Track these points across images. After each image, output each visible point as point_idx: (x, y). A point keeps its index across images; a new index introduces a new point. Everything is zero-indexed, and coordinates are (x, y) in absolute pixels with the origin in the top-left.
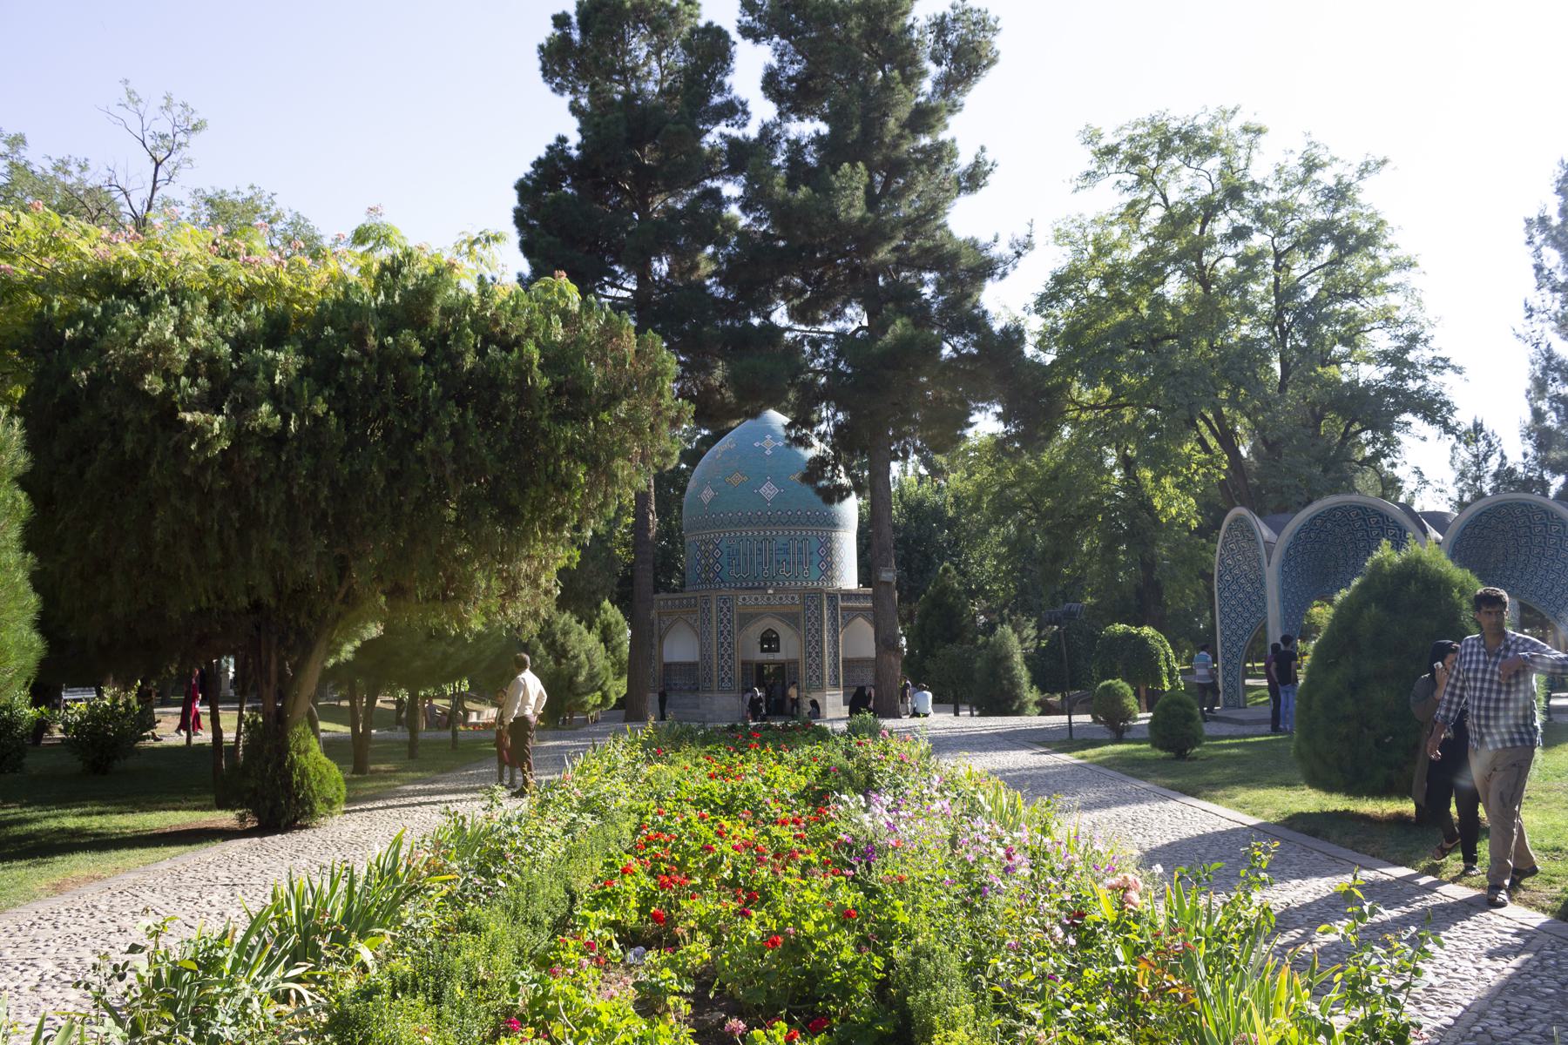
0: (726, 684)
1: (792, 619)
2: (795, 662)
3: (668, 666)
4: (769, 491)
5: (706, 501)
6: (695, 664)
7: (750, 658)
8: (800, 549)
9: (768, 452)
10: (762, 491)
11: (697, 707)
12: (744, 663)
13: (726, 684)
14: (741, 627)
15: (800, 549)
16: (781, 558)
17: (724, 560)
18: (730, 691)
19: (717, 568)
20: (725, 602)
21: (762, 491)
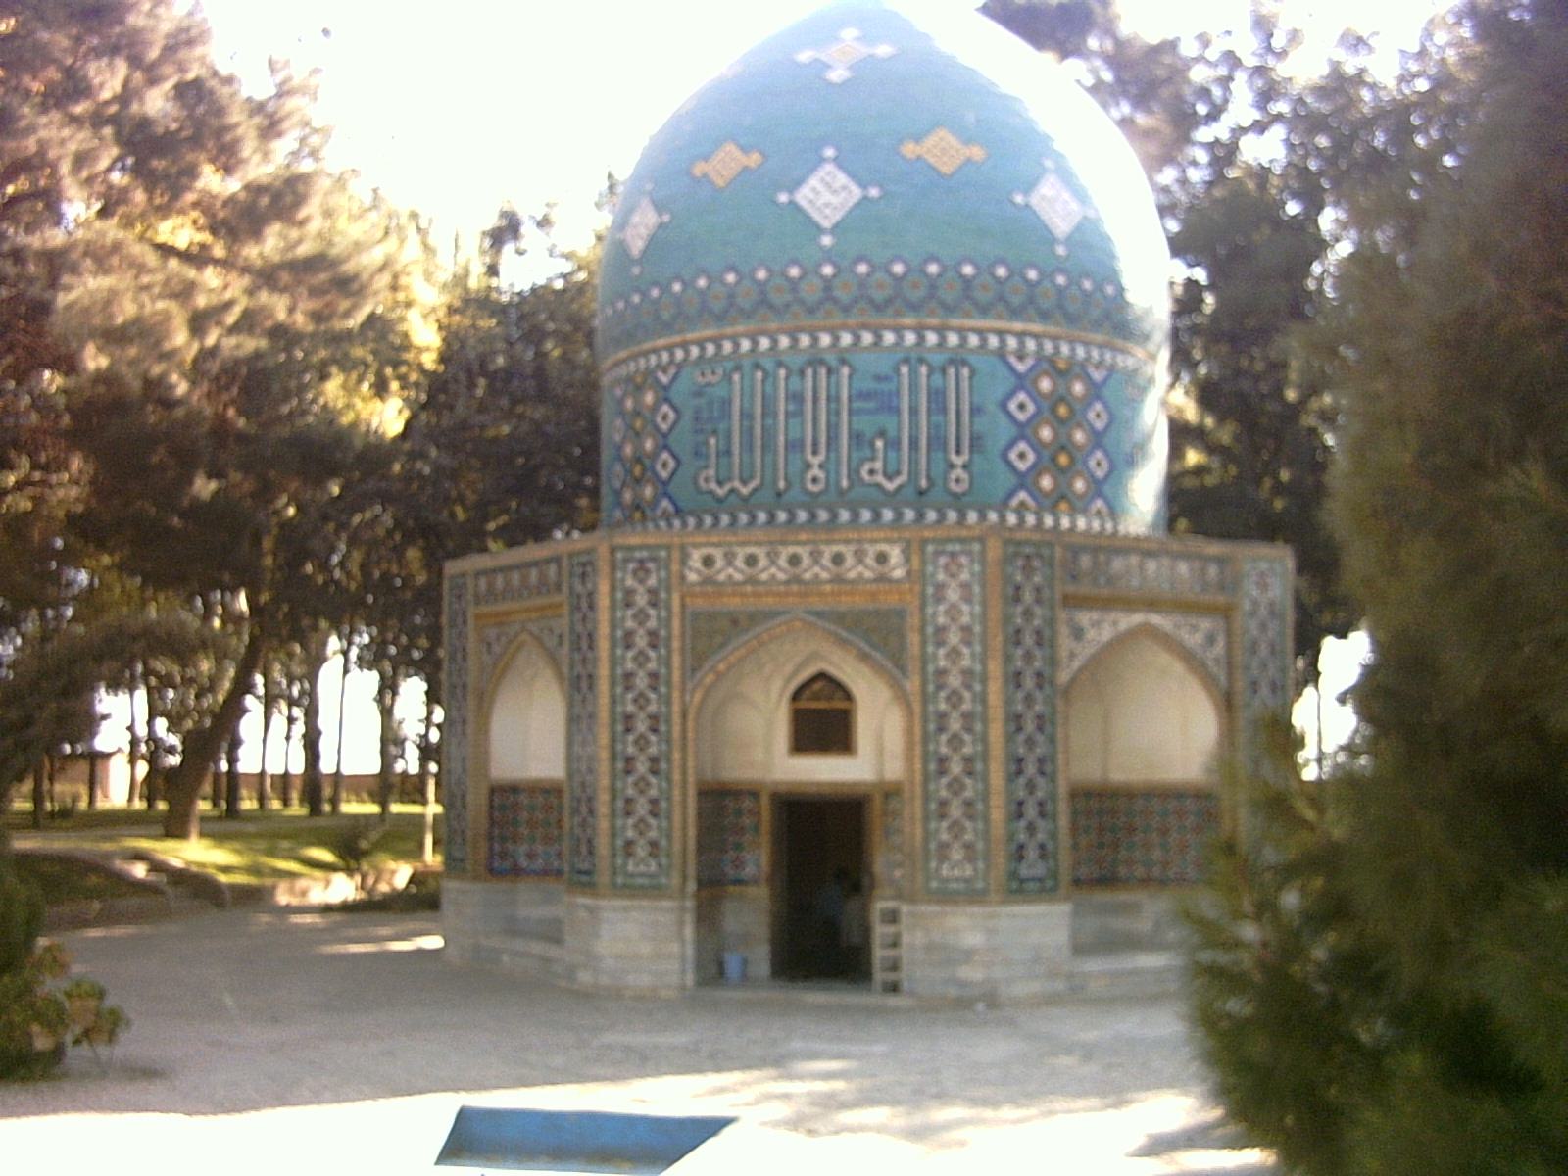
0: (641, 865)
2: (891, 792)
4: (828, 194)
5: (637, 246)
7: (739, 769)
8: (937, 398)
9: (837, 75)
10: (803, 196)
11: (553, 933)
13: (641, 865)
14: (696, 661)
15: (937, 398)
16: (866, 425)
17: (683, 440)
18: (652, 890)
21: (803, 196)
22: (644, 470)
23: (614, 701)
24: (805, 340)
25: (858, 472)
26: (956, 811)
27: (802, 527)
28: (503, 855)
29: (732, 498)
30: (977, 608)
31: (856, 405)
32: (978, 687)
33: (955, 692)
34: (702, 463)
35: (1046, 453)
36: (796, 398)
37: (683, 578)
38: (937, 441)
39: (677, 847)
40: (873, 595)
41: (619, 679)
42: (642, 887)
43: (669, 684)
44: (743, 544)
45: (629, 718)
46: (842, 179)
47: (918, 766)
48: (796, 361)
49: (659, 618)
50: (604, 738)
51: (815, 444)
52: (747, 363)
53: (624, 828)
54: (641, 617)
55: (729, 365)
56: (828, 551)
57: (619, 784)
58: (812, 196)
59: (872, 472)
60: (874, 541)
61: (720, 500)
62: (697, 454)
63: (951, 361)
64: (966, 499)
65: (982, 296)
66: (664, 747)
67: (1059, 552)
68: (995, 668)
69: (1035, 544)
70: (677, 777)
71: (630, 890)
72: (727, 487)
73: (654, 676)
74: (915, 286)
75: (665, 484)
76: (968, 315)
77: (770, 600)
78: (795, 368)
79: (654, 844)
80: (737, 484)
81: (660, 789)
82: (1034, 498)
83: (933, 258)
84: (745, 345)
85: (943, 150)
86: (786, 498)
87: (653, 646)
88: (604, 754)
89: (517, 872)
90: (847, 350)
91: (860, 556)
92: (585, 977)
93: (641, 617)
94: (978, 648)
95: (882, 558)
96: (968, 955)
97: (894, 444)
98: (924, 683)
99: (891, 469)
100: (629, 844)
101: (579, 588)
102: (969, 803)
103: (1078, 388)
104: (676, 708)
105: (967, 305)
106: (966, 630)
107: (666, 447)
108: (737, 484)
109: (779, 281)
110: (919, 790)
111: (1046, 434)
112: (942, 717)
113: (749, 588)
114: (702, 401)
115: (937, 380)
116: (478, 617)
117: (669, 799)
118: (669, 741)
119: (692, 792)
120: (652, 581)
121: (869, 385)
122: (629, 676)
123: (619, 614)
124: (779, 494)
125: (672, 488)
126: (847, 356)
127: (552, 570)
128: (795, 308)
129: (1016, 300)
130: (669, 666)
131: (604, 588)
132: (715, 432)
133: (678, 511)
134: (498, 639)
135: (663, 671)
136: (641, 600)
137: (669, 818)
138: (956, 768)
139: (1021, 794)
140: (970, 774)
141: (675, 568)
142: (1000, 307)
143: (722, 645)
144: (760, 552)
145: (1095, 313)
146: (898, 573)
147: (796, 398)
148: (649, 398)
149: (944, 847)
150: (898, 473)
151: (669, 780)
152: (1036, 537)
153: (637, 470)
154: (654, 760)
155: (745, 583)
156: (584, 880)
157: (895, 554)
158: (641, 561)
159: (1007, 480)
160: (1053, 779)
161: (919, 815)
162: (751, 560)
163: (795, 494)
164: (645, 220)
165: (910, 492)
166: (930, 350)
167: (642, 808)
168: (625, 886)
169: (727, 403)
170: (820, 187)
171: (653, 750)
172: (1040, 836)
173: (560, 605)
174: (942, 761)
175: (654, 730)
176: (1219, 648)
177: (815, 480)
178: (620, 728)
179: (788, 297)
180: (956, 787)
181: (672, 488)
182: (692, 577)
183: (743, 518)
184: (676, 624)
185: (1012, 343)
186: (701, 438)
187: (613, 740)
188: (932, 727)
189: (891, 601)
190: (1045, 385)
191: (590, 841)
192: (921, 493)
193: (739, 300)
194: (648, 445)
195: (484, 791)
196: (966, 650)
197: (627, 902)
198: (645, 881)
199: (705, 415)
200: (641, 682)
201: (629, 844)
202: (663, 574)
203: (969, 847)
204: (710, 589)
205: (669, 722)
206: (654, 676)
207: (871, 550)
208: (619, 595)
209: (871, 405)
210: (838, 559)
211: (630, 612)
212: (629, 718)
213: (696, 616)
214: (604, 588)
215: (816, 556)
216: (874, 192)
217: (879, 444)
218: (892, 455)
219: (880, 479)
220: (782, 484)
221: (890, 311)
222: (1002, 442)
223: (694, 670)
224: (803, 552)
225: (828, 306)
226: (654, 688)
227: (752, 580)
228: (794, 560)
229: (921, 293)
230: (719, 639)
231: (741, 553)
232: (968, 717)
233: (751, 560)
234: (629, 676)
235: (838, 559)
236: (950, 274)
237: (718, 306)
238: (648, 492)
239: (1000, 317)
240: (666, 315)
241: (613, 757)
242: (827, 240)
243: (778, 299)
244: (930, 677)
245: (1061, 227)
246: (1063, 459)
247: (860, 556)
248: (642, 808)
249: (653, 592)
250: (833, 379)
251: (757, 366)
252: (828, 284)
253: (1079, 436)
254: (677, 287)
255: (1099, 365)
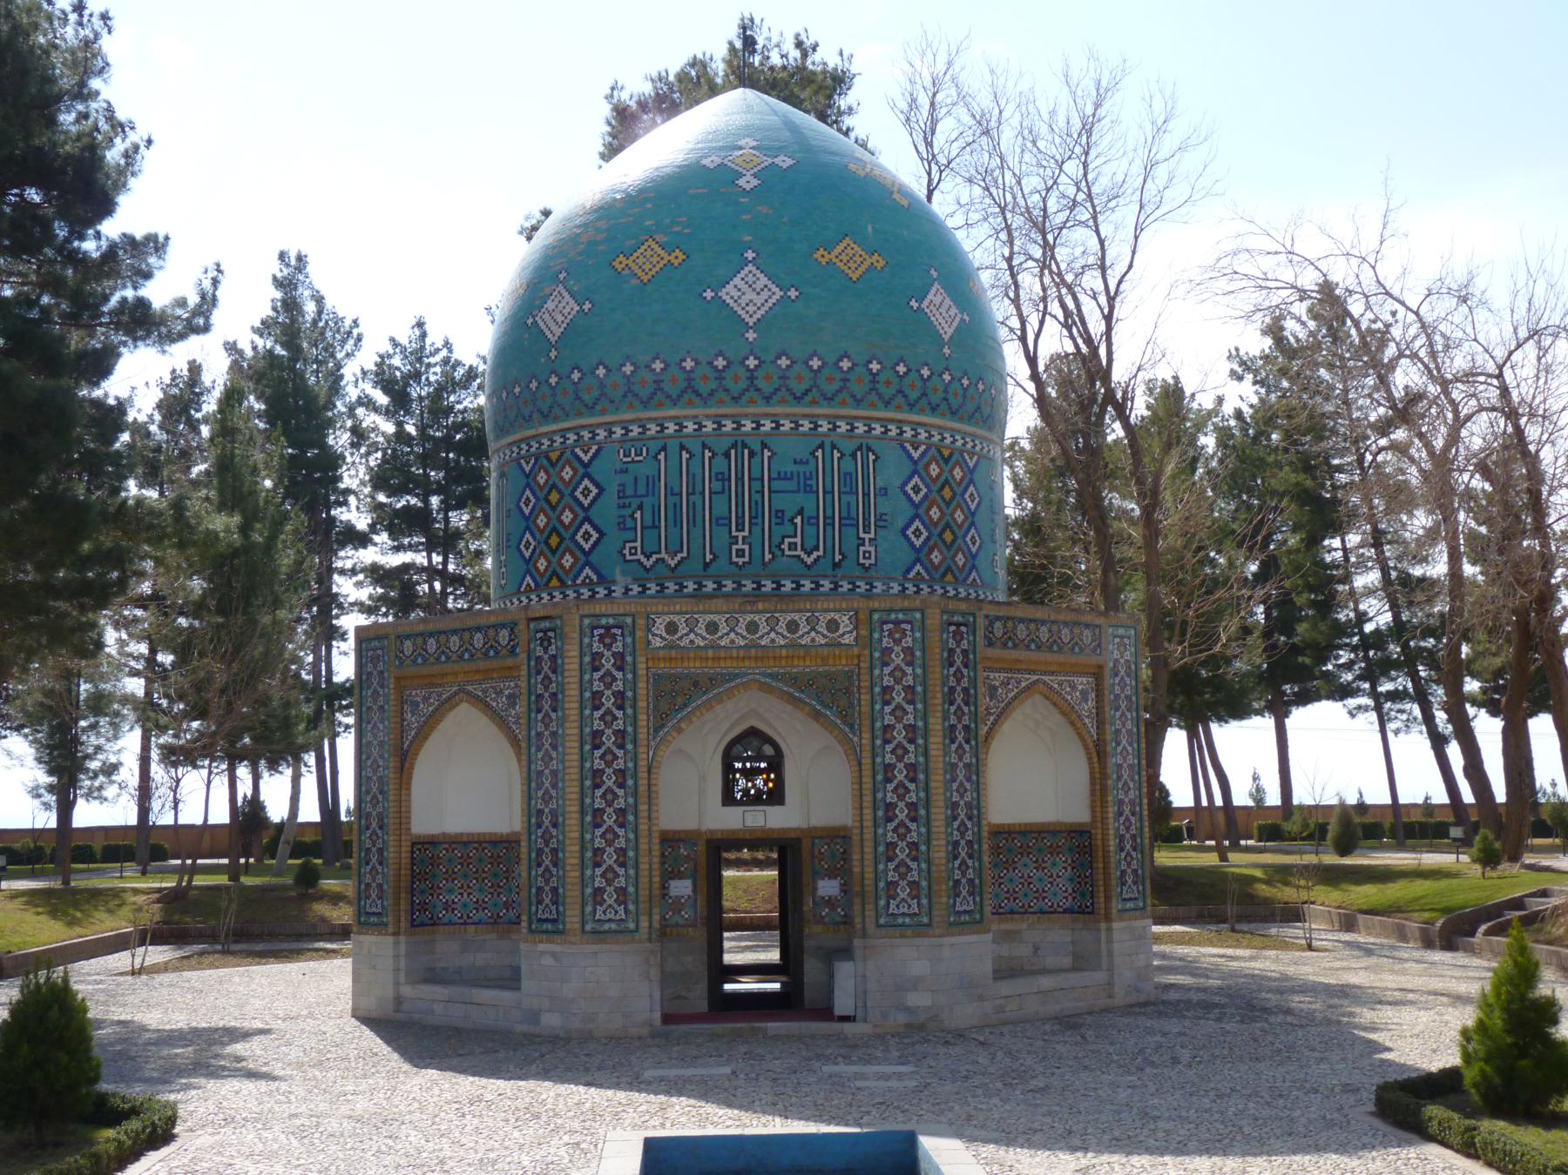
0: (610, 912)
1: (830, 695)
2: (837, 837)
3: (426, 847)
4: (750, 293)
5: (554, 332)
6: (507, 843)
8: (848, 478)
9: (748, 182)
10: (728, 293)
11: (511, 979)
12: (670, 840)
13: (610, 912)
15: (848, 478)
16: (788, 503)
17: (607, 512)
19: (585, 537)
20: (607, 635)
21: (728, 293)
22: (562, 539)
23: (582, 760)
24: (729, 426)
25: (779, 547)
26: (902, 853)
27: (710, 597)
28: (424, 907)
29: (660, 567)
30: (919, 671)
31: (777, 485)
32: (920, 741)
33: (899, 745)
34: (630, 535)
35: (936, 532)
36: (723, 478)
37: (649, 642)
38: (848, 520)
39: (644, 894)
40: (824, 660)
41: (588, 739)
42: (609, 931)
43: (635, 742)
44: (704, 613)
45: (597, 774)
46: (764, 280)
47: (868, 812)
48: (722, 444)
49: (625, 680)
50: (572, 791)
51: (740, 518)
52: (673, 446)
53: (593, 878)
54: (608, 679)
55: (655, 446)
56: (784, 619)
57: (588, 836)
58: (736, 294)
59: (793, 546)
60: (827, 611)
61: (647, 570)
62: (622, 526)
63: (860, 448)
64: (872, 573)
65: (888, 392)
66: (631, 800)
67: (981, 622)
68: (936, 724)
69: (963, 614)
70: (643, 827)
71: (599, 935)
72: (655, 557)
73: (621, 734)
74: (830, 380)
75: (587, 554)
76: (873, 406)
77: (729, 664)
78: (720, 450)
79: (622, 892)
80: (663, 555)
81: (627, 840)
82: (926, 570)
83: (846, 355)
84: (672, 428)
85: (850, 257)
86: (712, 570)
87: (621, 707)
88: (574, 808)
89: (434, 922)
90: (767, 434)
91: (813, 624)
92: (551, 1021)
93: (608, 679)
94: (920, 706)
95: (833, 625)
96: (915, 984)
97: (812, 521)
98: (873, 738)
99: (808, 546)
100: (598, 892)
101: (539, 652)
102: (913, 846)
103: (958, 473)
104: (643, 763)
105: (873, 397)
106: (910, 689)
107: (587, 519)
108: (663, 555)
109: (704, 369)
110: (868, 836)
111: (935, 513)
112: (889, 768)
113: (710, 653)
114: (627, 479)
115: (848, 465)
116: (398, 679)
117: (637, 849)
118: (635, 795)
119: (656, 840)
120: (618, 647)
121: (791, 468)
122: (597, 734)
123: (587, 677)
124: (706, 566)
125: (593, 558)
126: (768, 440)
127: (504, 635)
128: (722, 395)
129: (914, 395)
130: (635, 725)
131: (572, 652)
132: (640, 507)
133: (603, 580)
134: (425, 699)
135: (630, 729)
136: (608, 664)
137: (636, 867)
138: (902, 814)
139: (956, 836)
140: (914, 820)
141: (639, 634)
142: (900, 400)
143: (685, 706)
144: (721, 620)
145: (970, 406)
146: (847, 640)
147: (723, 478)
148: (567, 473)
149: (891, 885)
150: (817, 548)
151: (636, 832)
152: (963, 606)
153: (554, 541)
154: (621, 812)
155: (706, 647)
156: (552, 928)
157: (845, 623)
158: (608, 628)
159: (907, 556)
160: (979, 825)
161: (869, 856)
162: (712, 628)
163: (722, 561)
164: (560, 310)
165: (826, 565)
166: (842, 436)
167: (610, 859)
168: (594, 932)
169: (652, 482)
170: (741, 284)
171: (620, 803)
172: (970, 874)
173: (517, 668)
174: (890, 807)
175: (621, 786)
176: (1091, 704)
177: (740, 553)
178: (588, 783)
179: (713, 385)
180: (902, 830)
181: (593, 558)
182: (657, 642)
183: (672, 587)
184: (642, 685)
185: (909, 433)
186: (627, 512)
187: (582, 795)
188: (880, 777)
189: (842, 665)
190: (934, 470)
191: (555, 890)
192: (836, 566)
193: (666, 386)
194: (567, 517)
195: (406, 847)
196: (909, 708)
197: (596, 948)
198: (613, 926)
199: (629, 492)
200: (609, 741)
201: (598, 892)
202: (629, 640)
203: (914, 885)
204: (673, 653)
205: (635, 776)
206: (621, 734)
207: (824, 619)
208: (587, 659)
209: (792, 485)
210: (793, 626)
211: (597, 675)
212: (597, 774)
213: (658, 678)
214: (572, 652)
215: (773, 624)
216: (793, 294)
217: (798, 520)
218: (810, 530)
219: (799, 552)
220: (709, 557)
221: (808, 398)
222: (900, 524)
223: (656, 731)
224: (761, 619)
225: (752, 393)
226: (621, 746)
227: (714, 646)
228: (752, 627)
229: (836, 385)
230: (680, 700)
231: (703, 620)
232: (912, 768)
233: (712, 628)
234: (597, 734)
235: (793, 626)
236: (860, 370)
237: (644, 393)
238: (568, 561)
239: (899, 408)
240: (587, 398)
241: (583, 812)
242: (751, 336)
243: (705, 390)
244: (878, 733)
245: (948, 331)
246: (948, 536)
247: (813, 624)
248: (610, 859)
249: (619, 657)
250: (757, 459)
251: (682, 447)
252: (752, 375)
253: (959, 516)
254: (601, 371)
255: (972, 455)
